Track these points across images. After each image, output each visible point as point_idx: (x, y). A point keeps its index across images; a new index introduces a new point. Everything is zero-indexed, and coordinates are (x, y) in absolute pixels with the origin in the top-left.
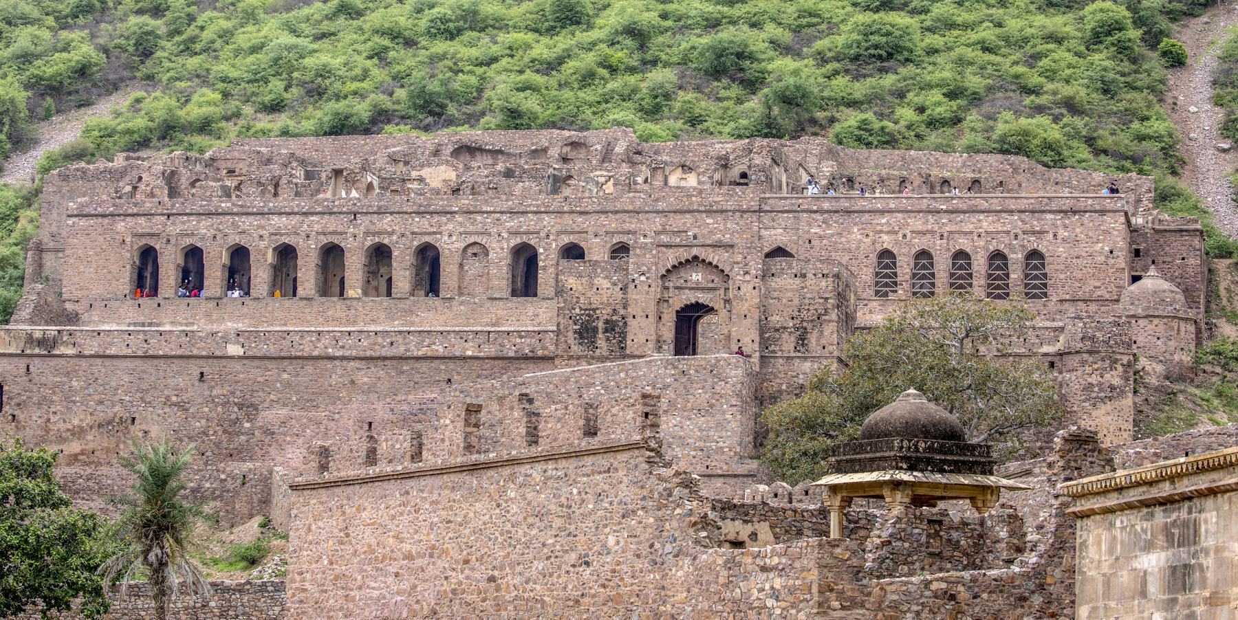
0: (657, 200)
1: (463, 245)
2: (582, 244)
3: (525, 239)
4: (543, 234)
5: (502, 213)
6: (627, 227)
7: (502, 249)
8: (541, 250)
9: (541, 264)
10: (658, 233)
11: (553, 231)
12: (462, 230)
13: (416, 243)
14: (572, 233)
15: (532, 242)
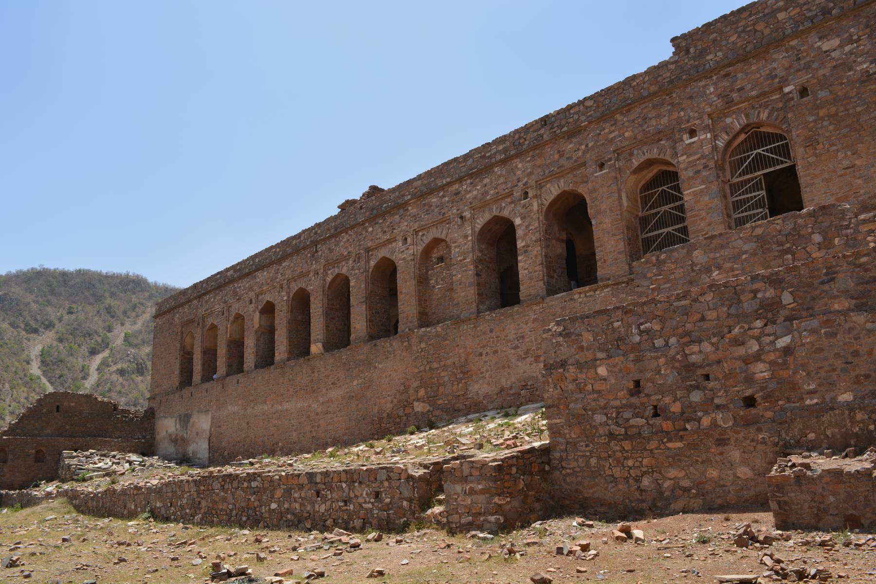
0: (703, 53)
1: (420, 248)
2: (582, 190)
3: (495, 212)
4: (517, 194)
5: (460, 180)
6: (652, 126)
7: (466, 237)
8: (518, 221)
9: (520, 244)
10: (717, 117)
11: (532, 182)
12: (416, 226)
13: (372, 263)
14: (561, 175)
15: (506, 213)
